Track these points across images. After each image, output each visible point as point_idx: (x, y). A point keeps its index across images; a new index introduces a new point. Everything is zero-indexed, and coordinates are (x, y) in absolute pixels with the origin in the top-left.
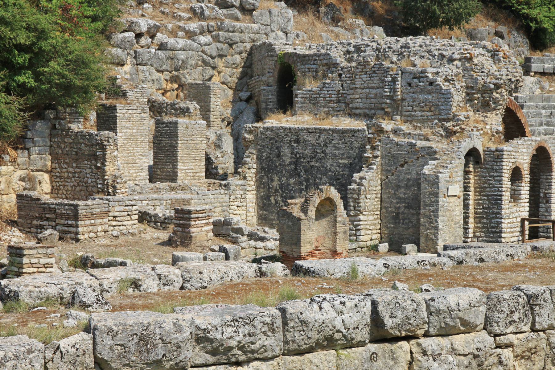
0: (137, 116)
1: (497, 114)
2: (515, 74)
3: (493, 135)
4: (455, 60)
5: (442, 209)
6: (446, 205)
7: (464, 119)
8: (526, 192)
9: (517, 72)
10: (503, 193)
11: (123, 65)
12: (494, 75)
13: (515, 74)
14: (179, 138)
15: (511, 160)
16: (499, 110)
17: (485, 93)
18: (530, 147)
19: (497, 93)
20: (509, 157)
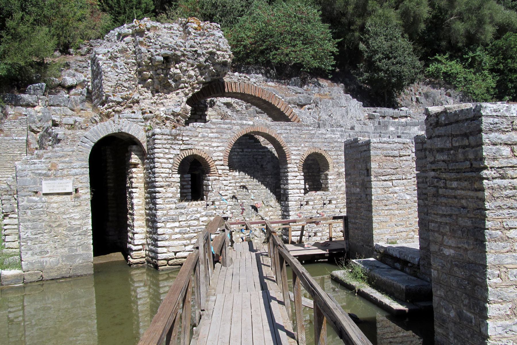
1: (177, 94)
2: (205, 45)
3: (167, 119)
4: (126, 36)
5: (29, 212)
7: (121, 100)
9: (209, 43)
10: (157, 189)
11: (34, 106)
12: (169, 47)
13: (205, 45)
15: (177, 147)
16: (182, 88)
17: (158, 69)
18: (229, 131)
19: (176, 68)
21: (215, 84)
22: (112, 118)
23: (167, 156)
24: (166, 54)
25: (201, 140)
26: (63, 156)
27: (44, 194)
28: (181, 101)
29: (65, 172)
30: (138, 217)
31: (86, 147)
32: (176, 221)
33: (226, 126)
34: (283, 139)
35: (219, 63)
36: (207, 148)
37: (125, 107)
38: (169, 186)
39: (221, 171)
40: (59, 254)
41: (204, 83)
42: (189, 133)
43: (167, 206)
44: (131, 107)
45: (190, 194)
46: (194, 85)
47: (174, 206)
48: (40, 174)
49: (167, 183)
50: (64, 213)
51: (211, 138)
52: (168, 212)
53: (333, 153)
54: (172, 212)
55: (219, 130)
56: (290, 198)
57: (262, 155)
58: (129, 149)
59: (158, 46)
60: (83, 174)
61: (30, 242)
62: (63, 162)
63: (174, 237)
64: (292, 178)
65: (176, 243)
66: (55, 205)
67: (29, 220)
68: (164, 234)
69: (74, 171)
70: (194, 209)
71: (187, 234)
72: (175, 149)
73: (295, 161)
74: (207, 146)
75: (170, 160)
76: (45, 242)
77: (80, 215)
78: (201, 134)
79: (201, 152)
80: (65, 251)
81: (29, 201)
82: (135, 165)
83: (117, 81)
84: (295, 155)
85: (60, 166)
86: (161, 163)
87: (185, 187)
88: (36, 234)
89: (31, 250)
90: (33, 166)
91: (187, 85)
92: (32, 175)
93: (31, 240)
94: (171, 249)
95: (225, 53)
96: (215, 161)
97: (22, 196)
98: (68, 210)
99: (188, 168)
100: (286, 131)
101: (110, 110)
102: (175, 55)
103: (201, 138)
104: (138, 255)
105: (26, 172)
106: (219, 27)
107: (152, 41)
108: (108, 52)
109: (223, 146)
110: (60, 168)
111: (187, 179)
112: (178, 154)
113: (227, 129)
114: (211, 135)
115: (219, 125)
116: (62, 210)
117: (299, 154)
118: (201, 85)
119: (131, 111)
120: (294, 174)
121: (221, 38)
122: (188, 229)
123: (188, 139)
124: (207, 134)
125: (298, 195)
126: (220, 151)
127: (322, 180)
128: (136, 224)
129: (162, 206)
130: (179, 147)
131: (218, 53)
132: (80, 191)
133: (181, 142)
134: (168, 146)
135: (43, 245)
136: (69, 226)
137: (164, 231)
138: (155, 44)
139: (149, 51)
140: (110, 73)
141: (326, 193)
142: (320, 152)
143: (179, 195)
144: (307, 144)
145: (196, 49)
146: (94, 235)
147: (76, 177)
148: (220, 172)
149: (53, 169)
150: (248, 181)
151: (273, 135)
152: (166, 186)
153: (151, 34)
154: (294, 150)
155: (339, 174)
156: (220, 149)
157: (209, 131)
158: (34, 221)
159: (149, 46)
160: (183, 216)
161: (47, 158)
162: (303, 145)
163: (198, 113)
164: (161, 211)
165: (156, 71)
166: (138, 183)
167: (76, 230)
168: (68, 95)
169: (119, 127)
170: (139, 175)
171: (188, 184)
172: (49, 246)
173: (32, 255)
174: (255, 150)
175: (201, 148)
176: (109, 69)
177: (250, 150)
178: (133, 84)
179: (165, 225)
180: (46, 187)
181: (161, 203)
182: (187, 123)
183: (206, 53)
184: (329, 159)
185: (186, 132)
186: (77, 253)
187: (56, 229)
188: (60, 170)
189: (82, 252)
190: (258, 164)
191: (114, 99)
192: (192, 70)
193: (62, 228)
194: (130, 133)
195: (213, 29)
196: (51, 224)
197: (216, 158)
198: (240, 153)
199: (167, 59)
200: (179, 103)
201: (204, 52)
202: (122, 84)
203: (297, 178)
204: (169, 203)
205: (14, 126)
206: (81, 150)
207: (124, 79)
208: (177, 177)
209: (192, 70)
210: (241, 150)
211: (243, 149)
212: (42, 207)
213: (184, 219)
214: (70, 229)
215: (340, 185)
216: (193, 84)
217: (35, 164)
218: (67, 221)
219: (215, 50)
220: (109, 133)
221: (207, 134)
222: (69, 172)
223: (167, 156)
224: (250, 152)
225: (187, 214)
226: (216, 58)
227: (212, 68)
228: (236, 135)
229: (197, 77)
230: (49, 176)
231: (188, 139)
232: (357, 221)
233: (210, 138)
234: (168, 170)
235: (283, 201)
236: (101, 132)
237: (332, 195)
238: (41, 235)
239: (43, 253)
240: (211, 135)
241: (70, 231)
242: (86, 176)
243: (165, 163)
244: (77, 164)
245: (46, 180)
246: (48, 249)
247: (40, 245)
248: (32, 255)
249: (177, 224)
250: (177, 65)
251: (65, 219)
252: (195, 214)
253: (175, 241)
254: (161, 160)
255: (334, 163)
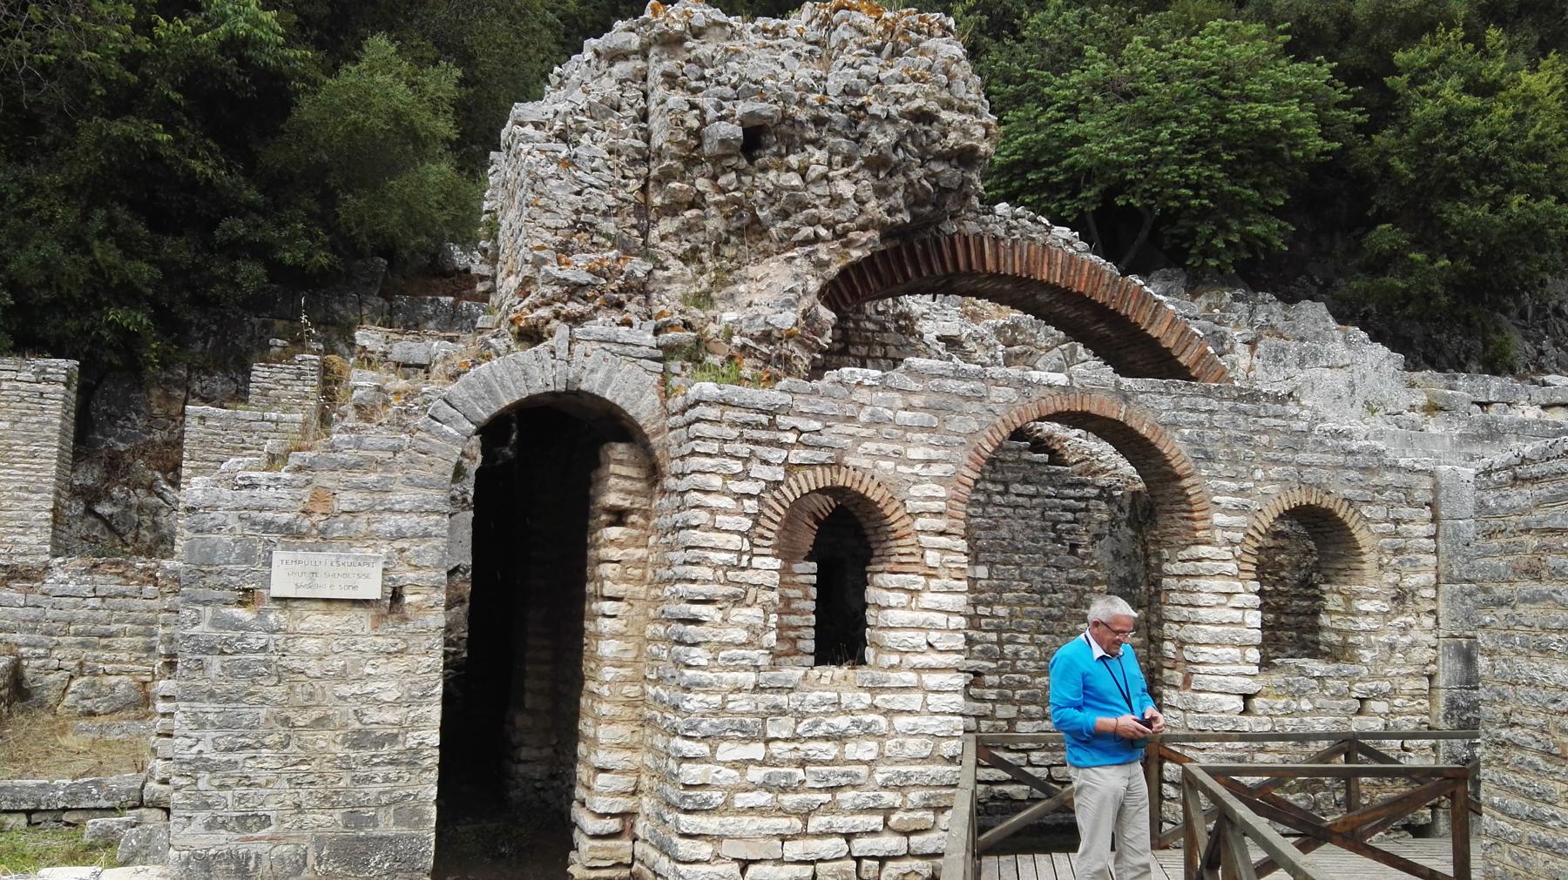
0: (17, 389)
5: (215, 663)
6: (255, 640)
8: (940, 619)
14: (185, 455)
15: (776, 455)
17: (724, 172)
20: (748, 433)
21: (923, 242)
22: (550, 342)
23: (737, 487)
24: (752, 114)
25: (865, 432)
26: (357, 465)
27: (275, 599)
28: (800, 290)
29: (361, 524)
30: (618, 710)
31: (445, 436)
32: (753, 740)
33: (964, 387)
34: (1182, 446)
35: (941, 157)
36: (887, 465)
37: (598, 302)
38: (737, 600)
39: (937, 554)
40: (308, 833)
41: (888, 232)
42: (824, 405)
43: (726, 676)
44: (619, 305)
45: (812, 631)
46: (852, 235)
47: (749, 678)
48: (267, 526)
49: (730, 590)
50: (342, 676)
51: (907, 428)
52: (725, 701)
53: (1379, 512)
54: (741, 703)
55: (935, 399)
56: (1199, 680)
57: (1074, 511)
58: (602, 459)
59: (728, 91)
60: (426, 535)
61: (208, 775)
62: (358, 488)
63: (742, 800)
64: (1213, 600)
65: (750, 824)
66: (311, 644)
67: (212, 695)
68: (704, 786)
69: (390, 523)
70: (828, 695)
71: (795, 791)
72: (766, 462)
73: (1228, 534)
74: (886, 457)
75: (746, 502)
76: (262, 781)
77: (401, 689)
78: (869, 409)
79: (866, 480)
80: (329, 820)
81: (217, 623)
82: (619, 516)
83: (577, 212)
84: (1225, 511)
85: (346, 500)
86: (713, 511)
87: (793, 606)
88: (231, 750)
89: (208, 806)
90: (245, 491)
91: (823, 232)
92: (238, 526)
93: (211, 768)
94: (728, 849)
95: (969, 118)
96: (915, 515)
97: (196, 602)
98: (357, 665)
99: (807, 539)
100: (1194, 417)
101: (544, 312)
102: (785, 117)
103: (867, 425)
104: (606, 854)
105: (219, 515)
106: (949, 29)
107: (708, 72)
108: (556, 113)
109: (947, 462)
110: (346, 507)
111: (802, 579)
112: (779, 483)
113: (968, 399)
114: (905, 416)
115: (936, 381)
116: (337, 664)
117: (1243, 510)
118: (873, 234)
119: (618, 319)
120: (1219, 584)
121: (958, 62)
122: (800, 773)
123: (817, 425)
124: (889, 413)
125: (1236, 669)
126: (938, 480)
127: (1328, 612)
128: (605, 733)
129: (706, 676)
130: (784, 453)
131: (945, 115)
132: (408, 599)
133: (791, 438)
134: (743, 449)
135: (253, 790)
136: (357, 725)
137: (706, 773)
138: (718, 83)
139: (693, 106)
140: (554, 182)
141: (1348, 668)
142: (1327, 502)
143: (773, 635)
144: (1274, 471)
145: (865, 99)
146: (443, 766)
147: (398, 544)
148: (932, 558)
149: (319, 508)
150: (1021, 602)
151: (1144, 431)
152: (727, 598)
153: (704, 49)
154: (1225, 492)
155: (1401, 597)
156: (937, 470)
157: (899, 403)
158: (228, 700)
159: (695, 91)
160: (782, 719)
161: (299, 469)
162: (1259, 474)
163: (853, 351)
164: (701, 696)
165: (715, 178)
166: (626, 581)
167: (379, 742)
168: (451, 299)
169: (572, 372)
170: (630, 550)
171: (806, 597)
172: (273, 799)
173: (210, 826)
174: (1050, 490)
175: (865, 463)
176: (553, 169)
177: (1032, 489)
178: (633, 226)
179: (714, 750)
180: (287, 573)
181: (703, 662)
182: (816, 371)
183: (902, 115)
184: (1364, 532)
185: (813, 399)
186: (377, 833)
187: (307, 735)
188: (345, 516)
189: (393, 831)
190: (1058, 539)
191: (562, 275)
192: (847, 176)
193: (328, 734)
194: (608, 396)
195: (930, 35)
196: (290, 713)
197: (918, 506)
198: (997, 499)
199: (755, 137)
200: (791, 296)
201: (893, 112)
202: (592, 225)
203: (1235, 601)
204: (733, 665)
205: (277, 382)
206: (423, 446)
207: (603, 207)
208: (767, 567)
209: (847, 176)
210: (1000, 488)
211: (1006, 484)
212: (264, 649)
213: (785, 734)
214: (359, 740)
215: (1407, 640)
216: (846, 231)
217: (253, 486)
218: (349, 708)
219: (933, 106)
220: (533, 391)
221: (889, 413)
222: (375, 526)
223: (737, 487)
224: (1031, 497)
225: (801, 716)
226: (935, 133)
227: (920, 172)
228: (998, 420)
229: (863, 203)
230: (300, 535)
231: (817, 425)
232: (1547, 810)
233: (899, 427)
234: (737, 538)
235: (1176, 687)
236: (503, 386)
237: (1373, 677)
238: (251, 753)
239: (250, 822)
240: (905, 416)
241: (356, 745)
242: (436, 542)
243: (726, 512)
244: (405, 496)
245: (287, 549)
246: (270, 809)
247: (241, 790)
248: (210, 826)
249: (757, 751)
250: (793, 160)
251: (344, 698)
252: (827, 714)
253: (746, 819)
254: (712, 501)
255: (1381, 551)
